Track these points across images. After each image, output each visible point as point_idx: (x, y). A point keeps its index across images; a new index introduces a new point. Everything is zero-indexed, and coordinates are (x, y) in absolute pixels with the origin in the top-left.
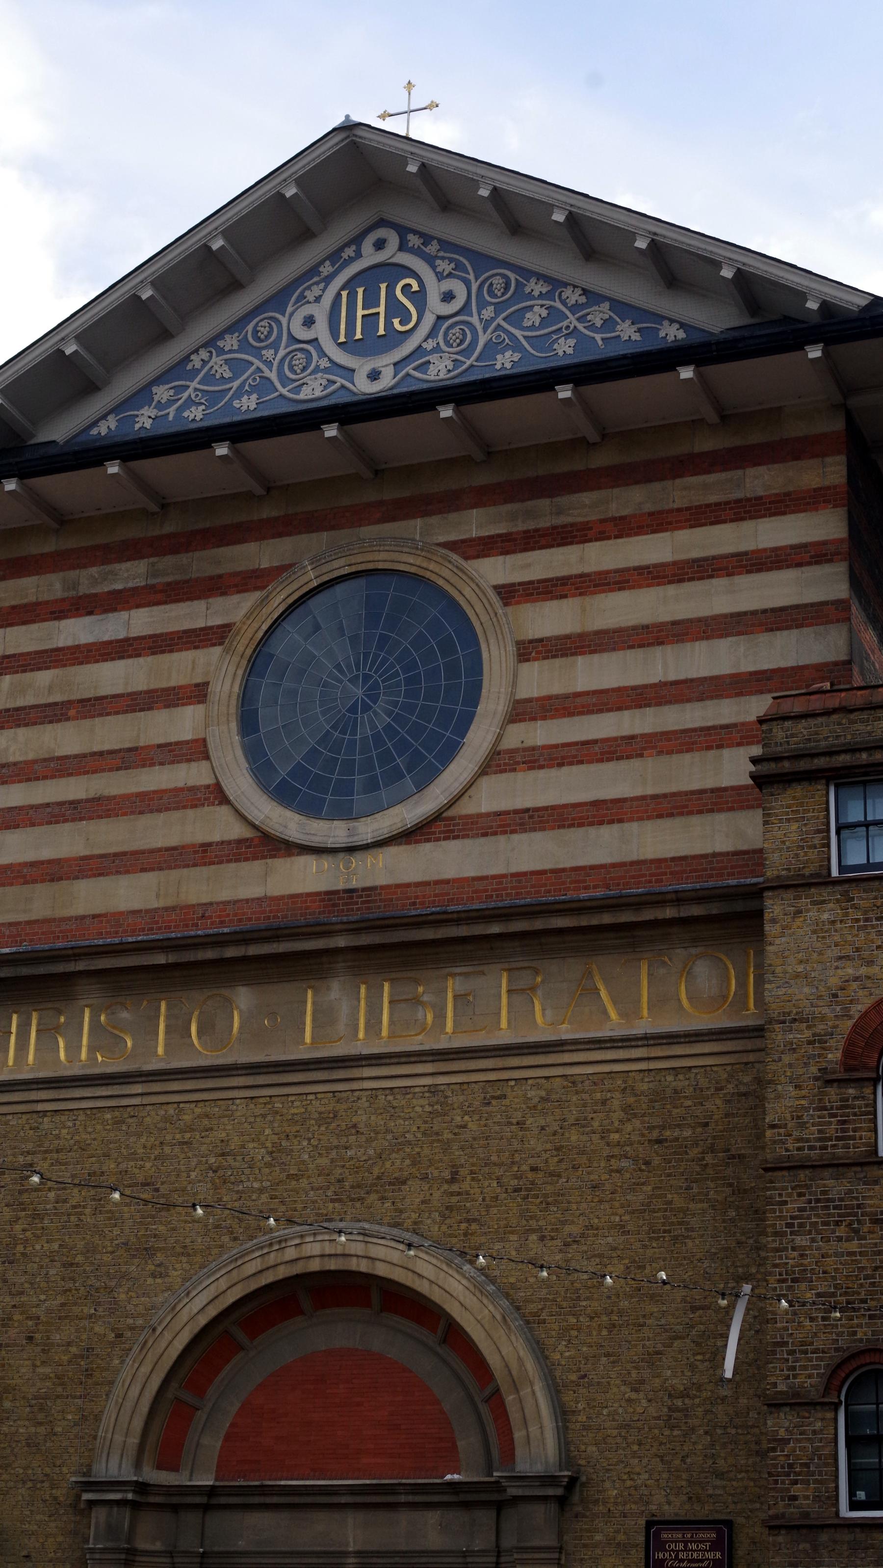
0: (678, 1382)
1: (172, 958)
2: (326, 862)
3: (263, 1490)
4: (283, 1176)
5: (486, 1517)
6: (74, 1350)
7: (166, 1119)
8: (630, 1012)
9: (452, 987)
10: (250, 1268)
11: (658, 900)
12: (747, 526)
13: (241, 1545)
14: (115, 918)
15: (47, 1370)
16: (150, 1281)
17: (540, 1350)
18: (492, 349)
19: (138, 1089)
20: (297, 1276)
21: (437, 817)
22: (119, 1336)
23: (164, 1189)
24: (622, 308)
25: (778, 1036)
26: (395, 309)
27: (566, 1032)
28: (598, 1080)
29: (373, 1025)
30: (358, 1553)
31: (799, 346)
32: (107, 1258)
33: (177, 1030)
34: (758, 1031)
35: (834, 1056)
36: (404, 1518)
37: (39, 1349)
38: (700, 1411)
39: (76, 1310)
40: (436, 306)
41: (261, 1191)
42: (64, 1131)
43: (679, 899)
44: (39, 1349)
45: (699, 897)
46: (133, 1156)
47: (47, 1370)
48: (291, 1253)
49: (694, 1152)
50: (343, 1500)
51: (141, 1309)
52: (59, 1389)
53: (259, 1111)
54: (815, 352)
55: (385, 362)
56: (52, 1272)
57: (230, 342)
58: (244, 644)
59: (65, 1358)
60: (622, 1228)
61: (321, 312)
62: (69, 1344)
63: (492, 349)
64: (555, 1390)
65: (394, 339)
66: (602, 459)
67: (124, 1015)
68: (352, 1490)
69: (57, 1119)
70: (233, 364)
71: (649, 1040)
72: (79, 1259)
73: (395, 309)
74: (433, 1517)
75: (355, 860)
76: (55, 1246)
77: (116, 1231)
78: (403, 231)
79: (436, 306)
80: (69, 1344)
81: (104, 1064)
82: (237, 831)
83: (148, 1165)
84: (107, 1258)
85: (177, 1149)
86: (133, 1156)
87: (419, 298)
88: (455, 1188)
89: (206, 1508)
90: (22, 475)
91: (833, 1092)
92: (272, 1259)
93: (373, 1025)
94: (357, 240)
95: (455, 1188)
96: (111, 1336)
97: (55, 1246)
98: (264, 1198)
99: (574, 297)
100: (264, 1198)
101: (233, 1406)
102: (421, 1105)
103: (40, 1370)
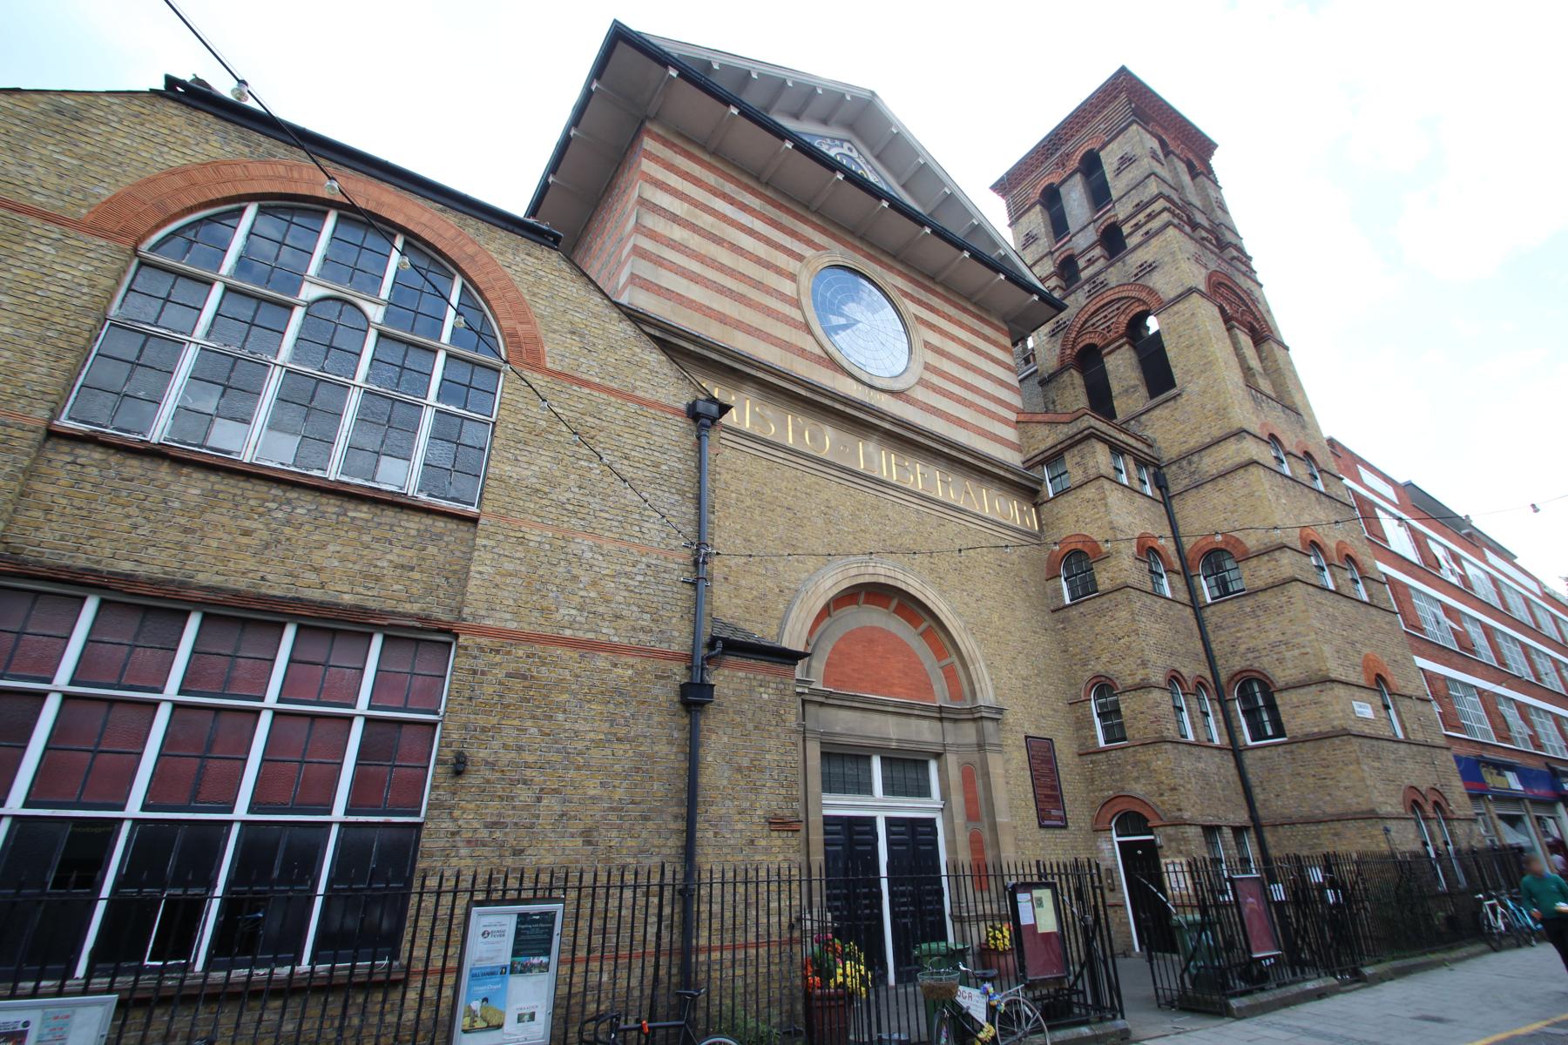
0: (1024, 673)
1: (809, 395)
2: (861, 387)
3: (853, 698)
4: (859, 529)
6: (755, 593)
7: (796, 477)
10: (853, 572)
13: (838, 729)
15: (739, 602)
16: (796, 564)
19: (782, 455)
20: (874, 583)
22: (781, 591)
23: (799, 515)
30: (899, 740)
32: (770, 543)
35: (1135, 549)
36: (914, 722)
37: (732, 587)
38: (1032, 687)
39: (754, 569)
41: (849, 533)
42: (739, 462)
44: (732, 587)
46: (779, 491)
47: (739, 602)
48: (871, 570)
49: (1012, 574)
50: (890, 709)
51: (793, 579)
52: (748, 615)
53: (843, 491)
56: (737, 542)
59: (750, 597)
62: (751, 589)
68: (896, 705)
69: (734, 452)
72: (753, 538)
74: (925, 723)
75: (873, 392)
76: (738, 527)
77: (774, 530)
80: (751, 589)
83: (789, 498)
84: (770, 543)
85: (804, 496)
86: (779, 491)
88: (932, 560)
89: (822, 704)
91: (1137, 562)
92: (863, 570)
94: (842, 141)
95: (932, 560)
96: (777, 590)
97: (738, 527)
98: (850, 537)
100: (850, 537)
101: (829, 648)
103: (734, 600)
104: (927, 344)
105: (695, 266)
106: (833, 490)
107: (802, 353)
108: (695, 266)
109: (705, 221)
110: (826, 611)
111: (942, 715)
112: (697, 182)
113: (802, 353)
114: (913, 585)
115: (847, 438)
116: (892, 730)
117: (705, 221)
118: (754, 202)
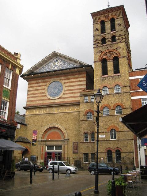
5: (63, 142)
8: (72, 110)
9: (61, 108)
11: (74, 103)
12: (80, 79)
14: (40, 104)
17: (66, 132)
18: (64, 66)
21: (60, 97)
24: (72, 64)
25: (81, 112)
26: (57, 63)
27: (68, 111)
28: (70, 114)
29: (56, 111)
31: (83, 67)
33: (44, 111)
34: (79, 112)
35: (84, 114)
40: (60, 63)
43: (75, 103)
45: (76, 103)
54: (84, 68)
55: (57, 67)
57: (47, 65)
58: (48, 86)
60: (71, 124)
61: (53, 64)
63: (64, 66)
64: (67, 134)
65: (57, 66)
66: (70, 74)
67: (40, 110)
70: (47, 67)
71: (73, 112)
73: (57, 63)
78: (58, 58)
79: (60, 63)
81: (39, 113)
82: (47, 98)
87: (59, 63)
90: (33, 75)
93: (56, 111)
99: (69, 63)
102: (59, 116)
104: (66, 87)
105: (33, 96)
106: (48, 117)
107: (45, 100)
108: (33, 96)
109: (35, 88)
110: (46, 131)
111: (62, 141)
112: (33, 84)
113: (45, 100)
114: (57, 125)
115: (50, 109)
116: (55, 143)
117: (35, 88)
118: (40, 81)
